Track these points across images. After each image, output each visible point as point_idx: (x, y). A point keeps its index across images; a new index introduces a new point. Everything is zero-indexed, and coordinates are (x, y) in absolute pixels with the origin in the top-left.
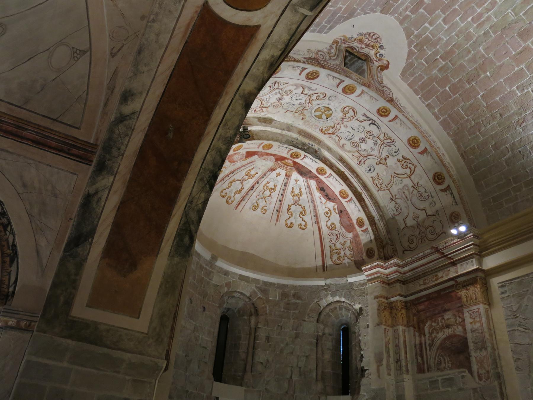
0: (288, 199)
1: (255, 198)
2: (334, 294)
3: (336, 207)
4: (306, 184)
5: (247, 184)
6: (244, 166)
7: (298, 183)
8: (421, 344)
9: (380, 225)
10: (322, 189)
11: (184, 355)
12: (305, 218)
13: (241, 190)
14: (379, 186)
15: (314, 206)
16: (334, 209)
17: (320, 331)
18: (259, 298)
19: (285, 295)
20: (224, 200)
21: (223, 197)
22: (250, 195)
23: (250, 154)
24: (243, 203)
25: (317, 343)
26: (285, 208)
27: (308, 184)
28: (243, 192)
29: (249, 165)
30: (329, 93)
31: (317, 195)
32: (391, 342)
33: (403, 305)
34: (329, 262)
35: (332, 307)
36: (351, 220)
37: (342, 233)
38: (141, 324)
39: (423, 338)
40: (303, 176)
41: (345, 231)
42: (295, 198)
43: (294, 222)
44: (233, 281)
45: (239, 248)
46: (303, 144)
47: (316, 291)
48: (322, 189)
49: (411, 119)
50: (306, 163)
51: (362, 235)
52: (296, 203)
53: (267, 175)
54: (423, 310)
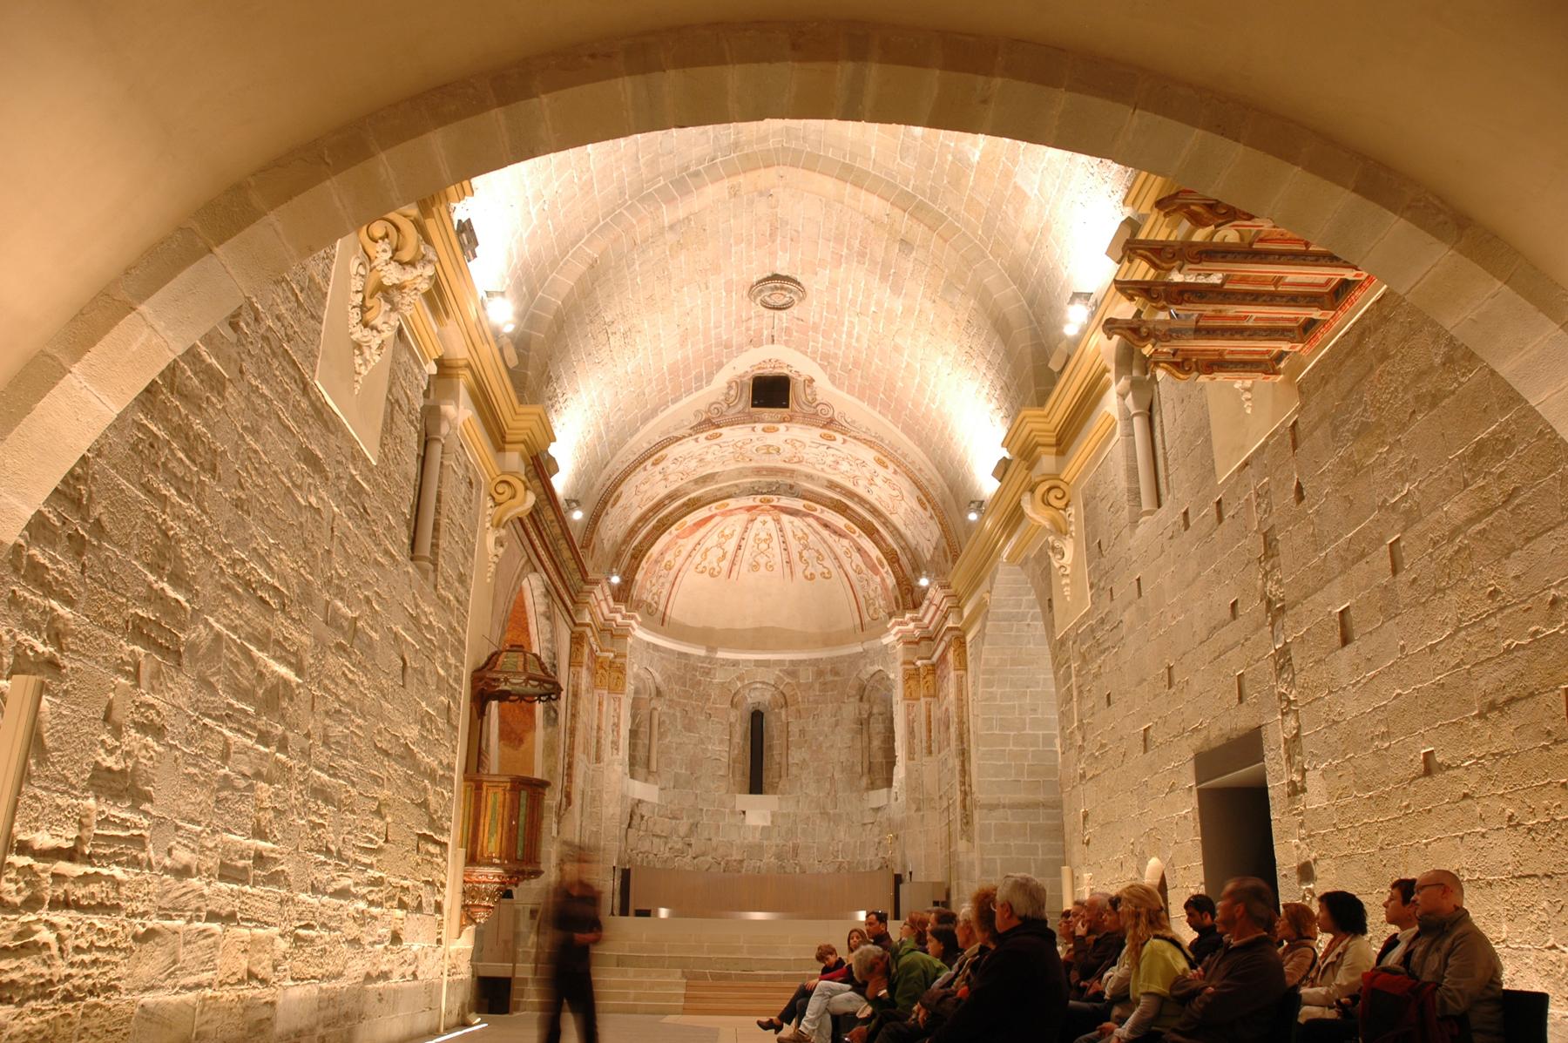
0: (795, 546)
2: (872, 663)
19: (820, 673)
20: (706, 575)
24: (736, 568)
26: (795, 557)
28: (729, 556)
30: (754, 437)
31: (825, 533)
34: (867, 619)
35: (877, 677)
45: (749, 624)
46: (770, 484)
47: (854, 660)
48: (826, 526)
49: (864, 436)
52: (806, 547)
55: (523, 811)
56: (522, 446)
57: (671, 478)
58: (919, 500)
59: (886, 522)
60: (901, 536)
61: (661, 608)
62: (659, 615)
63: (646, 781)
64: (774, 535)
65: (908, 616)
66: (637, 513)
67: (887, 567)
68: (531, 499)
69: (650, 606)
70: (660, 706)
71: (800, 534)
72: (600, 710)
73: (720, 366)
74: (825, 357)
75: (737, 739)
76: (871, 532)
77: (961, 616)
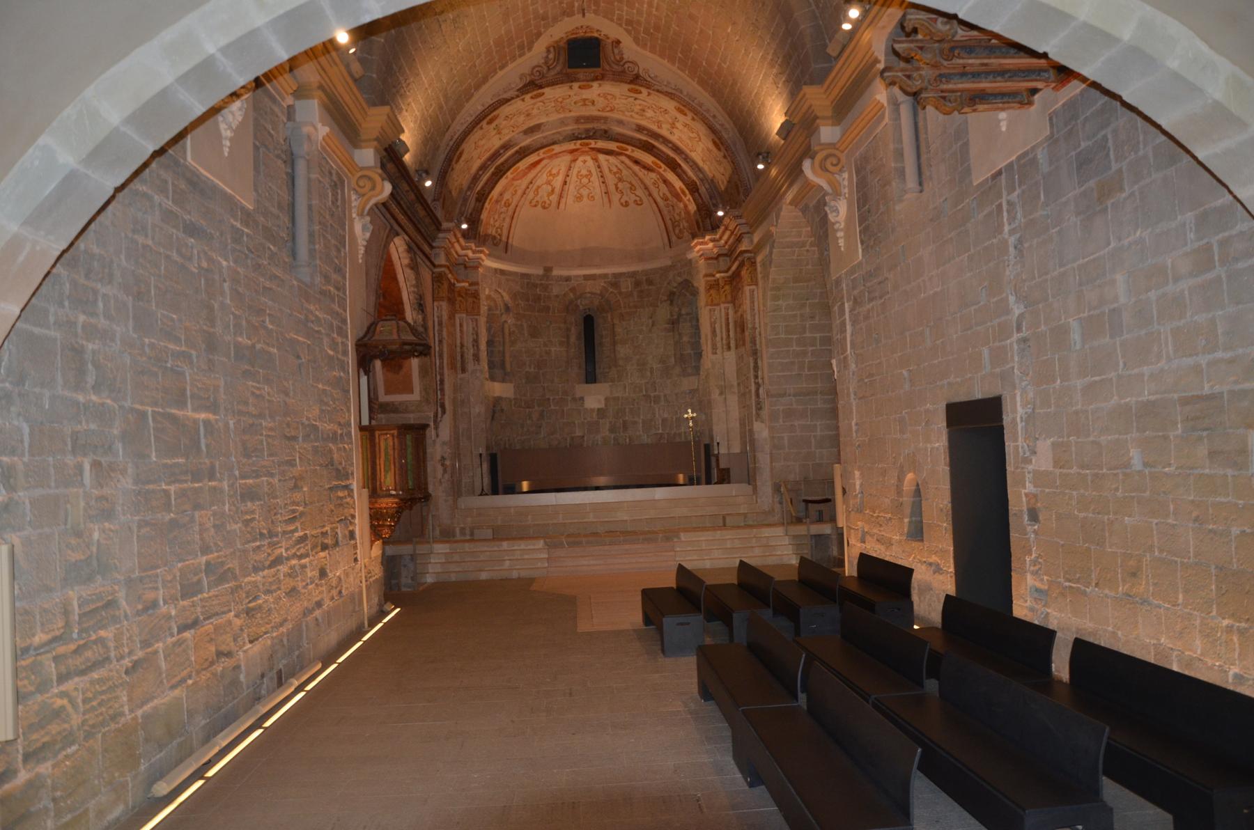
13: (553, 191)
19: (637, 284)
24: (563, 200)
26: (612, 188)
31: (636, 168)
38: (416, 396)
46: (587, 130)
48: (637, 162)
49: (665, 89)
52: (620, 180)
55: (410, 450)
56: (375, 143)
57: (505, 131)
58: (714, 143)
59: (687, 159)
60: (700, 170)
61: (504, 239)
62: (502, 246)
63: (503, 381)
64: (593, 171)
65: (707, 238)
66: (477, 164)
67: (689, 196)
68: (388, 188)
69: (494, 238)
71: (615, 170)
73: (539, 35)
74: (629, 22)
75: (573, 339)
76: (673, 166)
77: (752, 241)
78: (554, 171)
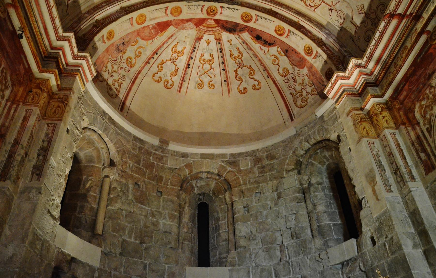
1: (196, 75)
3: (279, 49)
4: (241, 41)
5: (179, 63)
6: (165, 42)
7: (232, 43)
8: (418, 137)
9: (330, 42)
10: (258, 37)
11: (138, 242)
12: (256, 77)
14: (312, 4)
15: (260, 61)
16: (279, 52)
17: (304, 182)
18: (229, 171)
19: (258, 160)
20: (161, 84)
21: (158, 81)
22: (189, 74)
23: (163, 27)
24: (185, 84)
25: (305, 197)
26: (231, 75)
27: (242, 39)
28: (180, 72)
29: (170, 40)
31: (256, 46)
32: (381, 153)
33: (382, 108)
36: (300, 54)
37: (296, 73)
39: (418, 128)
40: (233, 33)
41: (298, 69)
42: (237, 61)
43: (246, 86)
44: (194, 161)
45: (196, 129)
48: (258, 38)
50: (227, 16)
51: (315, 62)
52: (240, 65)
53: (197, 47)
54: (406, 96)
61: (121, 96)
70: (113, 175)
72: (23, 126)
75: (186, 219)
78: (179, 49)
